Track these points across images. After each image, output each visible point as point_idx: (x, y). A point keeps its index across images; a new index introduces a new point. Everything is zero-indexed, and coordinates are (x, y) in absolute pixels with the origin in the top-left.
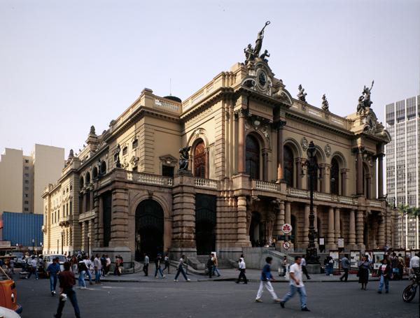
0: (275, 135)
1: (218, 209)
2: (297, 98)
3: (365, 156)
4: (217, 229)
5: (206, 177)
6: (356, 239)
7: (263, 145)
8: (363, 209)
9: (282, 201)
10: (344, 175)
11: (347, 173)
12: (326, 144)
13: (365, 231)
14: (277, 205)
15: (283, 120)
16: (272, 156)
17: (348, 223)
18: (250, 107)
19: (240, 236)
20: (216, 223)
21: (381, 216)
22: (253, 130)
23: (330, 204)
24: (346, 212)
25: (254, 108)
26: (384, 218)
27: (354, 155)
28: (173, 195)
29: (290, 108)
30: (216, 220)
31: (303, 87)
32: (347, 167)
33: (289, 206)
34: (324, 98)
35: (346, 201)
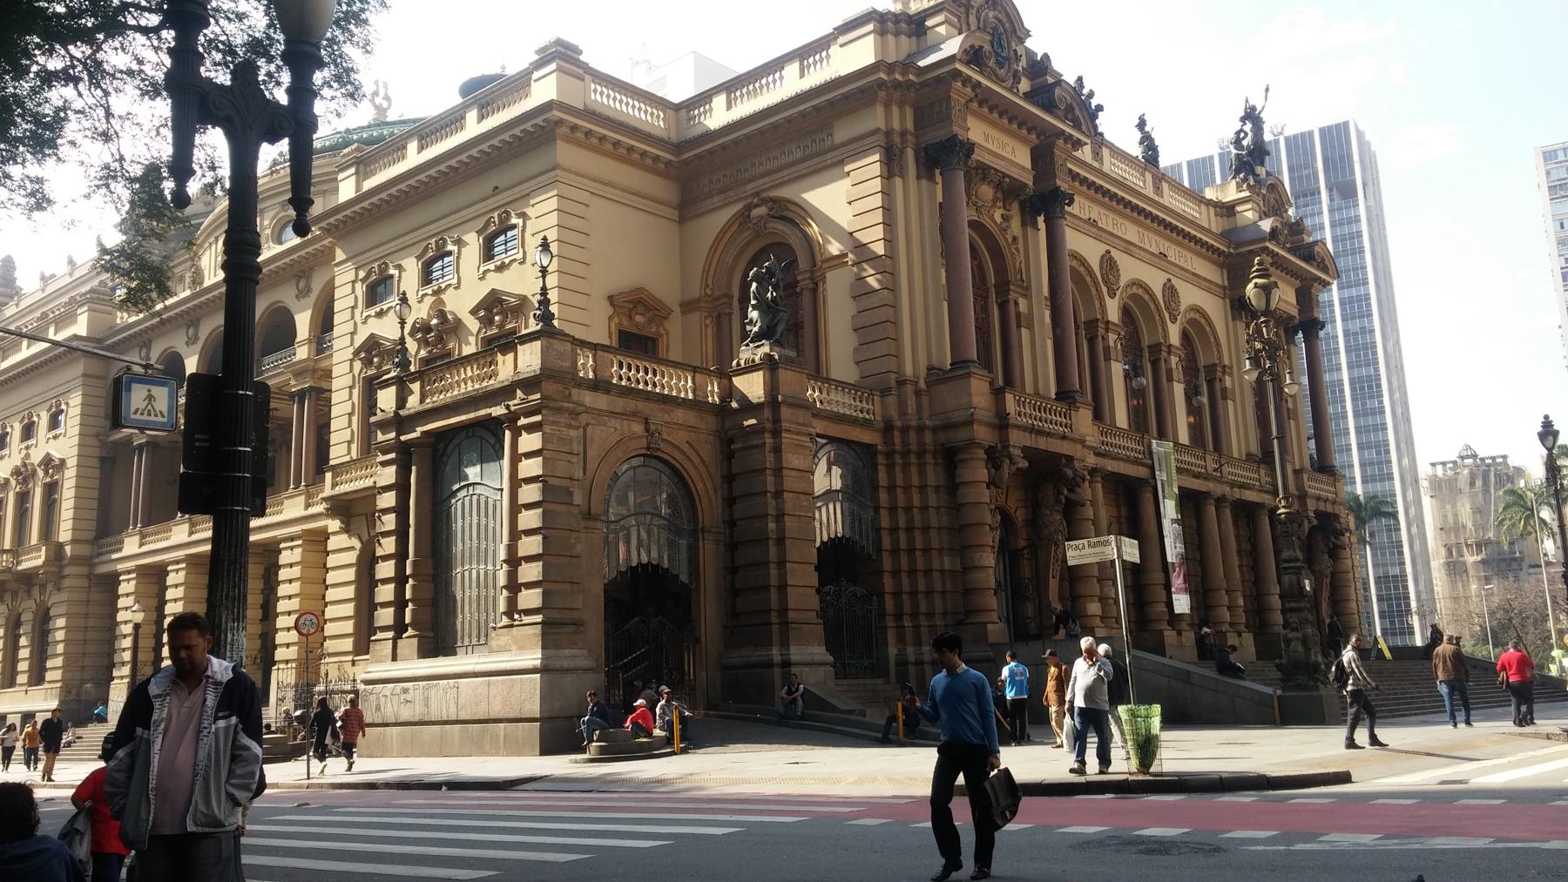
32: (1227, 362)
34: (1142, 124)
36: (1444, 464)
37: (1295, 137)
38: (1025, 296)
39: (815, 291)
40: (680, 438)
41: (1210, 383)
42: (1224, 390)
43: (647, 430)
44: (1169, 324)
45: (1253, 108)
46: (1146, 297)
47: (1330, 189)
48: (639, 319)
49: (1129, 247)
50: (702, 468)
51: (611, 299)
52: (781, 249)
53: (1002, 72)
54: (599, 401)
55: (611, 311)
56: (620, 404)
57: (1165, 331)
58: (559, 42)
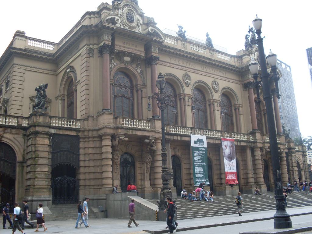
0: (149, 71)
1: (81, 151)
7: (137, 81)
8: (259, 145)
10: (237, 110)
11: (241, 109)
12: (213, 79)
18: (117, 43)
19: (105, 181)
20: (79, 167)
21: (281, 153)
22: (122, 65)
27: (246, 90)
29: (163, 44)
30: (79, 164)
32: (241, 103)
34: (207, 35)
39: (76, 91)
49: (195, 71)
51: (30, 98)
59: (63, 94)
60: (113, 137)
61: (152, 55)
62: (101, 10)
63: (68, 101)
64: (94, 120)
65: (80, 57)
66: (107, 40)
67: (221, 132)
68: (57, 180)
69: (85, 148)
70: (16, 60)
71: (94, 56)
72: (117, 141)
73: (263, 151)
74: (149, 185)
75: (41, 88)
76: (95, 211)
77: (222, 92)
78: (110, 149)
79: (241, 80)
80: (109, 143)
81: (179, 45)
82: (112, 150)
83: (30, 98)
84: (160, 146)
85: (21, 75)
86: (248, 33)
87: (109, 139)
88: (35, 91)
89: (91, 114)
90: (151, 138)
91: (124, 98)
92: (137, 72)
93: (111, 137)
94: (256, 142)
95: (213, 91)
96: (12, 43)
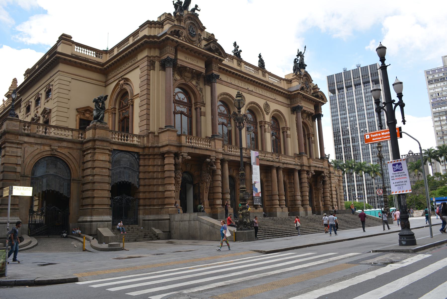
0: (208, 89)
2: (232, 54)
3: (305, 115)
4: (140, 192)
5: (130, 132)
6: (302, 201)
9: (217, 159)
13: (311, 192)
14: (211, 164)
15: (215, 73)
16: (208, 109)
17: (293, 184)
18: (179, 57)
19: (167, 201)
23: (271, 164)
24: (289, 172)
25: (183, 59)
26: (327, 179)
28: (84, 151)
31: (237, 44)
32: (288, 126)
33: (226, 166)
34: (260, 56)
35: (289, 161)
36: (405, 155)
37: (363, 67)
38: (204, 106)
39: (133, 105)
40: (65, 151)
41: (283, 132)
42: (287, 135)
43: (51, 148)
44: (266, 116)
45: (301, 53)
46: (257, 107)
47: (372, 81)
48: (87, 115)
49: (250, 92)
50: (73, 160)
51: (77, 109)
52: (127, 93)
53: (194, 39)
54: (32, 140)
55: (77, 113)
56: (39, 141)
57: (264, 117)
58: (63, 35)
59: (113, 108)
60: (176, 155)
61: (213, 73)
62: (164, 21)
63: (120, 115)
64: (155, 136)
65: (138, 69)
66: (169, 54)
67: (272, 154)
68: (116, 199)
69: (145, 166)
70: (61, 67)
71: (156, 69)
72: (180, 160)
73: (309, 175)
74: (208, 205)
75: (100, 100)
76: (158, 232)
77: (273, 114)
78: (173, 168)
79: (289, 103)
80: (172, 161)
81: (234, 64)
82: (176, 168)
83: (77, 109)
84: (220, 166)
85: (67, 83)
86: (296, 57)
87: (172, 157)
88: (94, 102)
89: (151, 130)
90: (212, 158)
91: (183, 115)
92: (197, 89)
93: (174, 154)
94: (304, 165)
95: (265, 113)
96: (55, 47)
